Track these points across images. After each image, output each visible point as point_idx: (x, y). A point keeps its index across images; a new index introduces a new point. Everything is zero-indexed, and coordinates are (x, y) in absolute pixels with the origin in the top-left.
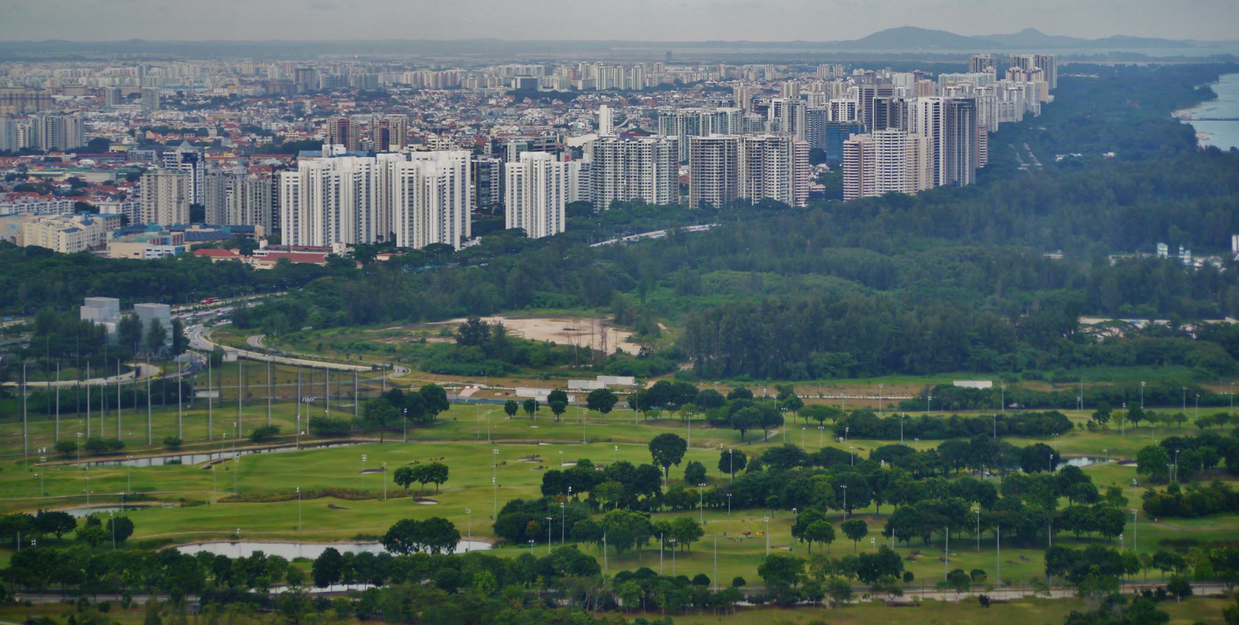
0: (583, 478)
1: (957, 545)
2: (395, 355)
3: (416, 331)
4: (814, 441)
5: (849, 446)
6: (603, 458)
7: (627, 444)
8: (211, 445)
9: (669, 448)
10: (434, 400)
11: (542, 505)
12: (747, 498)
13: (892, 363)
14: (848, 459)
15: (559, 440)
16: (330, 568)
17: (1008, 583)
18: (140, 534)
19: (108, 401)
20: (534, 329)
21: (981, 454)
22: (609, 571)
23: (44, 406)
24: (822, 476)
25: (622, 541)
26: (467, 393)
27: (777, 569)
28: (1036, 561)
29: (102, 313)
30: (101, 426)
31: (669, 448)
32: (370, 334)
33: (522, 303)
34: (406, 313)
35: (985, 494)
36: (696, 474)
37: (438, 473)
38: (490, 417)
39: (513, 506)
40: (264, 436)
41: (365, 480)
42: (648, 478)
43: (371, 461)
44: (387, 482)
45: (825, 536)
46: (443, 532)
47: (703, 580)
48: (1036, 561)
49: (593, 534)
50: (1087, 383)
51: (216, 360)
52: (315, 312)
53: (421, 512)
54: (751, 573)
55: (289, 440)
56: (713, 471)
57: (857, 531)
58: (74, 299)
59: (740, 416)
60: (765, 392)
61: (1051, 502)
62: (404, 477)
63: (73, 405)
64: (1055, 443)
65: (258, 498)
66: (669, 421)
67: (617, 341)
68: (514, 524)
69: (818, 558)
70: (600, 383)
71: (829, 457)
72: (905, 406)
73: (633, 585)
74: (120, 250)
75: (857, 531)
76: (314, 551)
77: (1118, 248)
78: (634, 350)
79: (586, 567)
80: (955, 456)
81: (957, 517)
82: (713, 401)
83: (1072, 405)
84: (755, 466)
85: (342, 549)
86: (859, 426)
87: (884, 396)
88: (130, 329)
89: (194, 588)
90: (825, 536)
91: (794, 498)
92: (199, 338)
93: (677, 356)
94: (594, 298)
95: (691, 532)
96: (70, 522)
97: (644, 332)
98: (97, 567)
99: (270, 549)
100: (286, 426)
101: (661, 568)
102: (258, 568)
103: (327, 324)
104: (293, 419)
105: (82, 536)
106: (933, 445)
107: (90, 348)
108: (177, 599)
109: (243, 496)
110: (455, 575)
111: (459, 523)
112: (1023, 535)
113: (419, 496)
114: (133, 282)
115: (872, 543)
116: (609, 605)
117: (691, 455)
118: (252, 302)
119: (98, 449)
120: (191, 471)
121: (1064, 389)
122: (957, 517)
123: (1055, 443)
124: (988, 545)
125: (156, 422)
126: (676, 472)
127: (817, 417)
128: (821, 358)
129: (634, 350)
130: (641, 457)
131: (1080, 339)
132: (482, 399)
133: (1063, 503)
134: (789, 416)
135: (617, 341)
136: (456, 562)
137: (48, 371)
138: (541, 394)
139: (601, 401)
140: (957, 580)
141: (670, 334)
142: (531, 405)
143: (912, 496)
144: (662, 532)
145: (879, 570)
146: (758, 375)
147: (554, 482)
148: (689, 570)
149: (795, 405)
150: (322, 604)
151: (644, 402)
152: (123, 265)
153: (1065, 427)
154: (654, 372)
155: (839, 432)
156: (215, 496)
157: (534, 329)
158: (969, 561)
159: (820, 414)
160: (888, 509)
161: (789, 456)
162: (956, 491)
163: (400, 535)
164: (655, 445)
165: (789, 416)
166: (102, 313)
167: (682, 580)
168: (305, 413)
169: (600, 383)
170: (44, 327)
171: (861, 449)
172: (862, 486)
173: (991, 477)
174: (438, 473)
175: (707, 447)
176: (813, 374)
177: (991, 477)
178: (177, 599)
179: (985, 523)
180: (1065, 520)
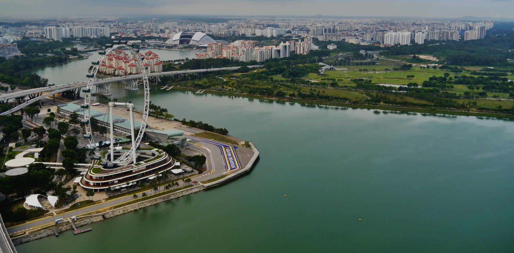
0: (434, 78)
1: (495, 92)
2: (403, 60)
3: (405, 56)
4: (468, 75)
5: (473, 76)
6: (438, 76)
7: (440, 74)
8: (379, 71)
9: (447, 75)
10: (410, 66)
11: (429, 82)
12: (460, 82)
13: (477, 64)
14: (474, 78)
15: (428, 72)
16: (400, 89)
17: (503, 98)
18: (372, 82)
19: (366, 64)
20: (422, 57)
21: (496, 79)
22: (441, 92)
23: (357, 64)
24: (472, 81)
25: (443, 87)
26: (414, 65)
27: (466, 93)
28: (507, 95)
29: (363, 52)
30: (365, 67)
31: (447, 75)
32: (399, 56)
33: (420, 53)
34: (403, 54)
35: (497, 84)
36: (451, 79)
37: (413, 76)
38: (418, 69)
39: (425, 82)
40: (387, 70)
41: (402, 77)
42: (445, 79)
43: (404, 74)
44: (406, 77)
45: (473, 89)
46: (416, 85)
47: (455, 94)
48: (507, 95)
49: (438, 86)
50: (509, 68)
51: (378, 59)
52: (391, 53)
53: (413, 81)
54: (462, 93)
55: (390, 70)
56: (453, 78)
57: (478, 88)
58: (359, 50)
59: (456, 71)
60: (459, 67)
61: (508, 86)
62: (408, 76)
63: (362, 64)
64: (507, 77)
65: (389, 78)
66: (445, 71)
67: (435, 59)
68: (425, 84)
69: (473, 92)
70: (433, 65)
71: (471, 77)
72: (481, 70)
73: (445, 94)
74: (362, 44)
75: (478, 88)
76: (398, 86)
77: (510, 49)
78: (438, 60)
79: (438, 91)
80: (492, 79)
81: (494, 88)
82: (451, 68)
83: (508, 72)
84: (459, 78)
85: (402, 86)
86: (475, 73)
87: (478, 69)
88: (366, 54)
89: (382, 90)
90: (473, 89)
91: (467, 83)
92: (374, 55)
93: (444, 62)
94: (430, 53)
95: (453, 87)
96: (363, 80)
97: (438, 58)
98: (368, 86)
99: (392, 86)
100: (390, 68)
101: (449, 92)
102: (390, 88)
103: (392, 55)
104: (391, 68)
105: (365, 82)
106: (487, 76)
107: (361, 57)
108: (380, 92)
109: (385, 78)
110: (418, 91)
111: (418, 84)
112: (505, 91)
113: (410, 79)
114: (366, 48)
115: (481, 90)
116: (442, 97)
117: (450, 76)
118: (382, 51)
119: (364, 70)
120: (377, 74)
121: (505, 69)
122: (494, 88)
123: (507, 77)
124: (500, 92)
125: (372, 67)
126: (448, 78)
127: (469, 71)
128: (466, 63)
129: (438, 60)
130: (443, 76)
131: (507, 62)
132: (415, 66)
133: (510, 87)
134: (463, 71)
135: (435, 59)
136: (419, 89)
137: (356, 60)
138: (425, 66)
139: (435, 67)
140: (495, 97)
141: (443, 59)
142: (424, 67)
143: (486, 84)
144: (448, 87)
145: (483, 95)
146: (456, 65)
147: (431, 79)
148: (453, 93)
149: (464, 69)
150: (400, 94)
151: (441, 68)
152: (364, 46)
153: (507, 75)
154: (441, 64)
155: (471, 74)
156: (382, 78)
157: (422, 57)
158: (497, 94)
159: (468, 71)
160: (481, 85)
161: (464, 77)
162: (493, 84)
163: (410, 85)
164: (445, 74)
165: (463, 71)
166: (363, 52)
167: (452, 94)
168: (392, 67)
169: (433, 65)
170: (355, 54)
171: (476, 76)
172: (478, 82)
173: (497, 82)
174: (413, 76)
175: (452, 75)
176: (465, 65)
177: (497, 82)
178: (380, 92)
179: (498, 89)
180: (511, 89)
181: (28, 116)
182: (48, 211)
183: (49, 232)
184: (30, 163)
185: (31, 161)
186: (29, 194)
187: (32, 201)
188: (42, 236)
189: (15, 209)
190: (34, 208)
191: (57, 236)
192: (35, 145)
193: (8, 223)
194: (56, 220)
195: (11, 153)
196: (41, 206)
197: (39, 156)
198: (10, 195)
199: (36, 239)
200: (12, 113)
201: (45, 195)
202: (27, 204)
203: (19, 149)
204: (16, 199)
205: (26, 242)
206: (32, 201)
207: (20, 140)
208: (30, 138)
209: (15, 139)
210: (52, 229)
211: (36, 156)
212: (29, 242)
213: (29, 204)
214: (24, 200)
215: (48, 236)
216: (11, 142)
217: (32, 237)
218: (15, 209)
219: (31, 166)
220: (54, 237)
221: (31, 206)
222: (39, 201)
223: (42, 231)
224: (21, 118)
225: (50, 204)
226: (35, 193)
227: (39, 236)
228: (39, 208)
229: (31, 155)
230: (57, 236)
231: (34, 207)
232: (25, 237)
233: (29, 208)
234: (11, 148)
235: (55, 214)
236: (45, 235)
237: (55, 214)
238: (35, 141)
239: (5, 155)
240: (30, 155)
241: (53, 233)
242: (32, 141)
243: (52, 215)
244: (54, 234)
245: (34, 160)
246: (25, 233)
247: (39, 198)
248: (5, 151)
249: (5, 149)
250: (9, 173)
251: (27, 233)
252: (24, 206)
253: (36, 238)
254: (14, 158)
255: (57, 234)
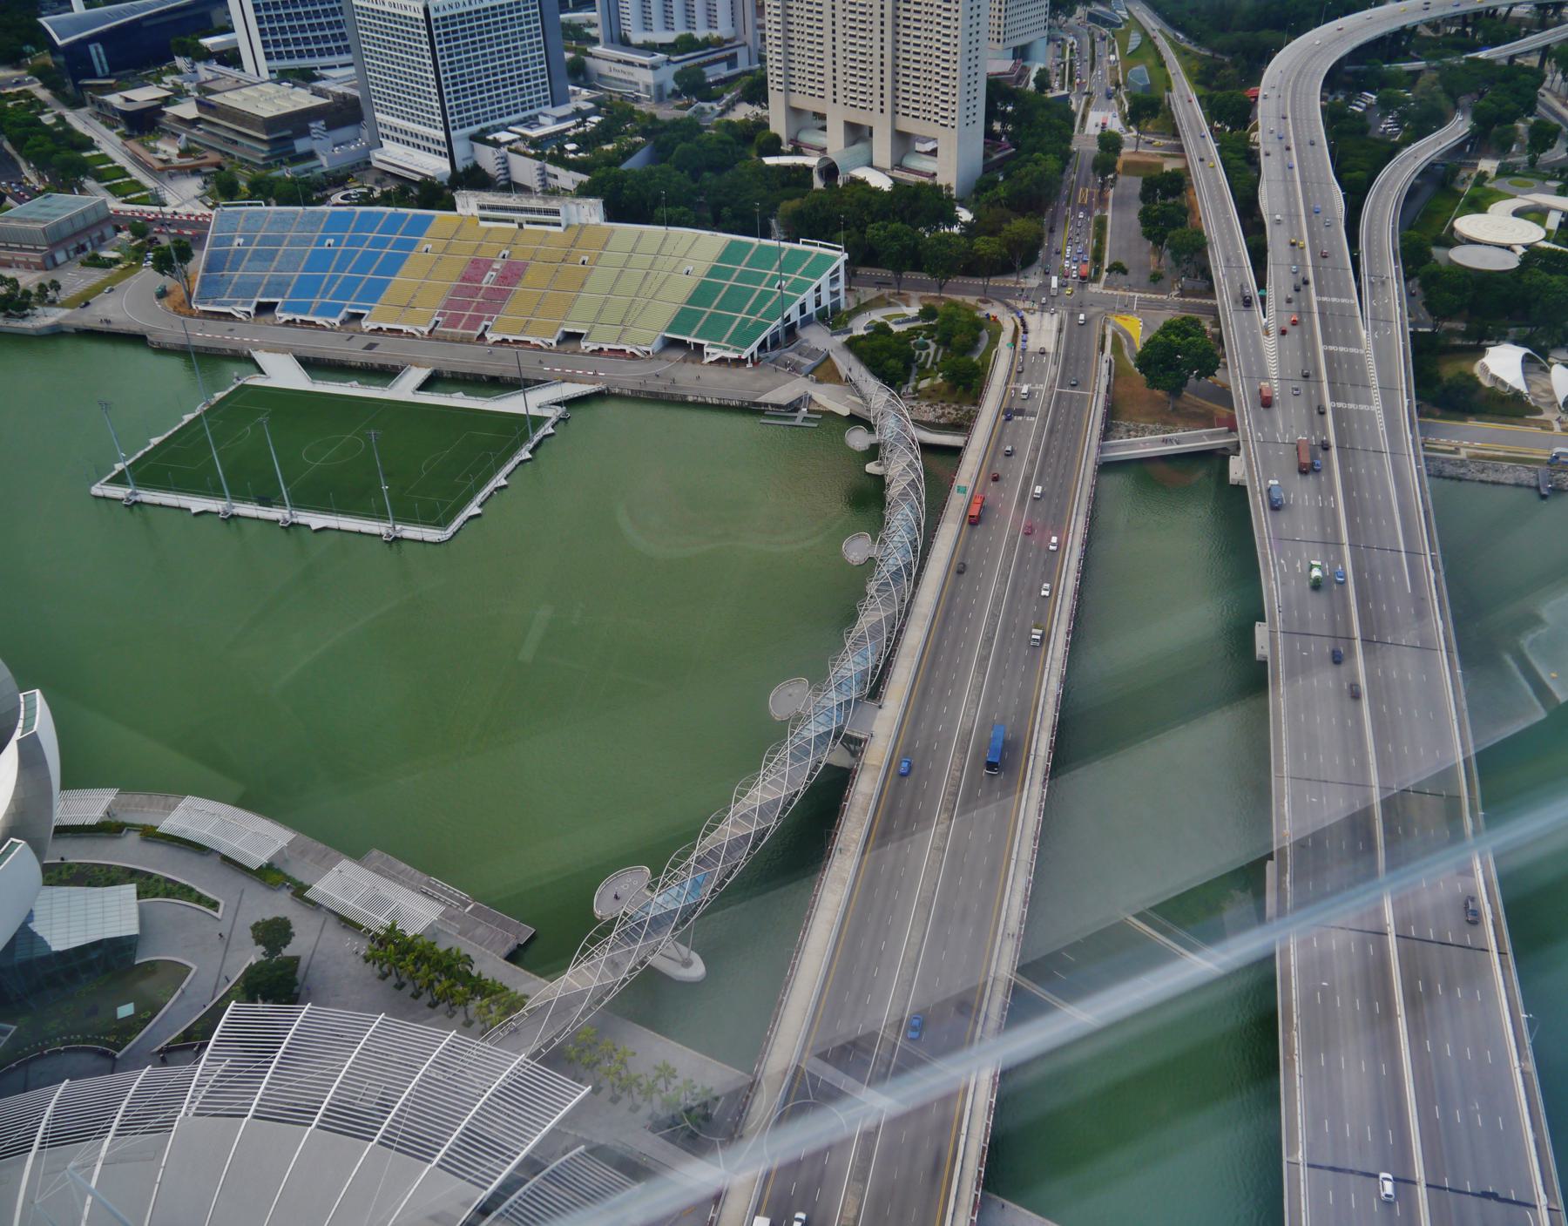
181: (1559, 77)
182: (1539, 412)
183: (1526, 476)
184: (1528, 241)
185: (1532, 234)
186: (1500, 337)
187: (1503, 363)
188: (1502, 478)
189: (1449, 370)
190: (1500, 388)
191: (1544, 497)
192: (1556, 184)
193: (1426, 408)
194: (1558, 450)
195: (1478, 191)
196: (1521, 386)
197: (1561, 224)
198: (1446, 324)
199: (1482, 481)
200: (1512, 58)
201: (1546, 357)
202: (1485, 369)
203: (1503, 184)
204: (1458, 342)
205: (1452, 478)
206: (1503, 363)
207: (1514, 155)
208: (1548, 157)
209: (1503, 149)
210: (1536, 471)
211: (1554, 220)
212: (1460, 480)
213: (1493, 371)
214: (1480, 351)
215: (1517, 485)
216: (1486, 154)
217: (1473, 472)
218: (1449, 370)
219: (1532, 251)
220: (1533, 495)
221: (1495, 379)
222: (1525, 372)
223: (1506, 465)
224: (1538, 76)
225: (1551, 392)
226: (1516, 343)
227: (1492, 476)
228: (1517, 395)
229: (1537, 214)
230: (1544, 497)
231: (1504, 383)
232: (1454, 463)
233: (1486, 383)
234: (1483, 176)
235: (1557, 427)
236: (1509, 478)
237: (1557, 427)
238: (1562, 171)
239: (1459, 195)
240: (1532, 216)
241: (1533, 483)
242: (1551, 166)
243: (1546, 425)
244: (1538, 488)
245: (1543, 234)
246: (1457, 451)
247: (1527, 360)
248: (1463, 182)
249: (1463, 174)
250: (1460, 255)
251: (1463, 454)
252: (1477, 369)
253: (1483, 476)
254: (1482, 210)
255: (1545, 492)
